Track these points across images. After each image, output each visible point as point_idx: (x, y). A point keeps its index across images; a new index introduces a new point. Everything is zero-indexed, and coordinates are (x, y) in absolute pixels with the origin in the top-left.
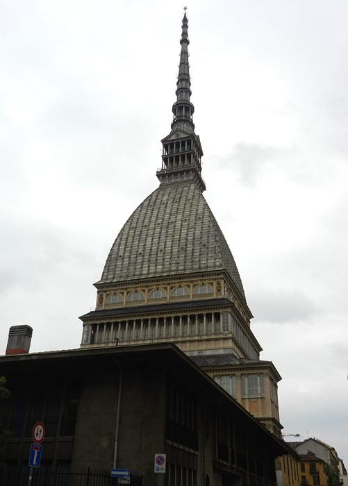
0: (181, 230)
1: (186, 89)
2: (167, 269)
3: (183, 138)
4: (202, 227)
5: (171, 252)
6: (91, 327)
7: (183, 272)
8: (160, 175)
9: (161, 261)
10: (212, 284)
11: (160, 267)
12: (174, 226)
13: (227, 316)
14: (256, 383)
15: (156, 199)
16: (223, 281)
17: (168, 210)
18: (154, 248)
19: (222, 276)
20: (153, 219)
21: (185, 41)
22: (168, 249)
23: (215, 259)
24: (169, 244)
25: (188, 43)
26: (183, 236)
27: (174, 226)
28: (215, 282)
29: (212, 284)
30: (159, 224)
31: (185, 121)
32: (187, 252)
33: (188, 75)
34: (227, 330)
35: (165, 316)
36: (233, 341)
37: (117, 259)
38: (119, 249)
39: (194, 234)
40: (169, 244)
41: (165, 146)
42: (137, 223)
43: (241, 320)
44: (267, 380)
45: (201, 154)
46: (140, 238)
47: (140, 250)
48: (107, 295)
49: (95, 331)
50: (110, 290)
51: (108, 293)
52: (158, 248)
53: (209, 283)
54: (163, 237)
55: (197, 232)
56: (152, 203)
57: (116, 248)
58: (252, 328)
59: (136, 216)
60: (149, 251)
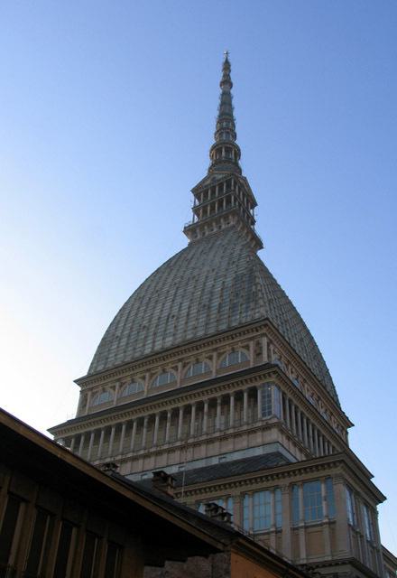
8: (189, 230)
10: (247, 347)
16: (265, 341)
20: (169, 280)
21: (227, 82)
24: (186, 304)
28: (252, 344)
29: (247, 347)
33: (231, 115)
34: (270, 413)
45: (254, 204)
48: (93, 394)
50: (97, 387)
54: (178, 300)
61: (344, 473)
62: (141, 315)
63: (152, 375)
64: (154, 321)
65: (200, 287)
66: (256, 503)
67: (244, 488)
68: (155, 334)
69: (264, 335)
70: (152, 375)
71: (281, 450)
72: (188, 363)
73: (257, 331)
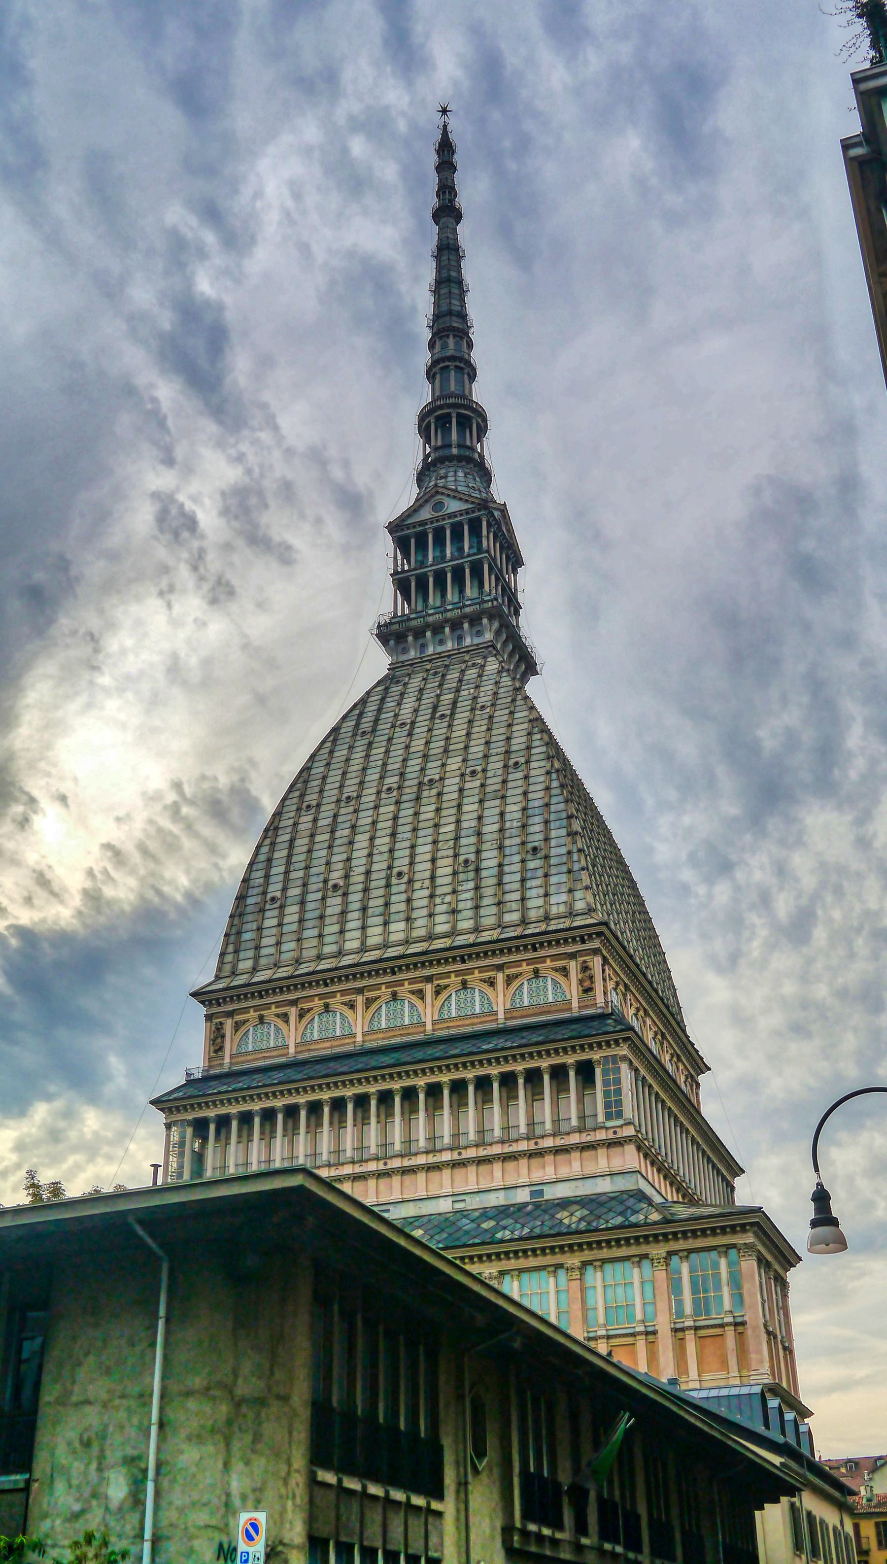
0: (459, 806)
1: (461, 359)
2: (422, 932)
4: (525, 793)
5: (433, 878)
6: (189, 1131)
7: (471, 938)
9: (403, 907)
10: (564, 971)
11: (398, 929)
12: (440, 794)
13: (618, 1070)
14: (717, 1276)
15: (380, 710)
16: (597, 961)
17: (418, 745)
18: (381, 864)
19: (596, 944)
20: (373, 776)
22: (423, 868)
23: (570, 891)
24: (424, 851)
25: (458, 216)
26: (469, 822)
27: (440, 794)
28: (573, 966)
29: (564, 971)
30: (389, 789)
31: (460, 459)
32: (484, 873)
34: (620, 1114)
35: (421, 1082)
36: (639, 1148)
37: (262, 911)
38: (267, 876)
39: (502, 814)
40: (424, 851)
41: (402, 544)
42: (321, 791)
43: (668, 1082)
44: (749, 1265)
45: (516, 561)
46: (333, 839)
47: (336, 876)
48: (237, 1026)
49: (205, 1139)
51: (238, 1018)
52: (390, 868)
53: (556, 970)
54: (404, 831)
55: (509, 808)
56: (366, 724)
57: (258, 876)
58: (709, 1110)
59: (318, 769)
60: (361, 878)
61: (757, 1243)
62: (321, 853)
63: (369, 1003)
64: (357, 878)
65: (449, 813)
66: (609, 1281)
67: (587, 1255)
68: (364, 909)
69: (596, 952)
70: (369, 1003)
71: (643, 1186)
72: (446, 987)
73: (583, 941)
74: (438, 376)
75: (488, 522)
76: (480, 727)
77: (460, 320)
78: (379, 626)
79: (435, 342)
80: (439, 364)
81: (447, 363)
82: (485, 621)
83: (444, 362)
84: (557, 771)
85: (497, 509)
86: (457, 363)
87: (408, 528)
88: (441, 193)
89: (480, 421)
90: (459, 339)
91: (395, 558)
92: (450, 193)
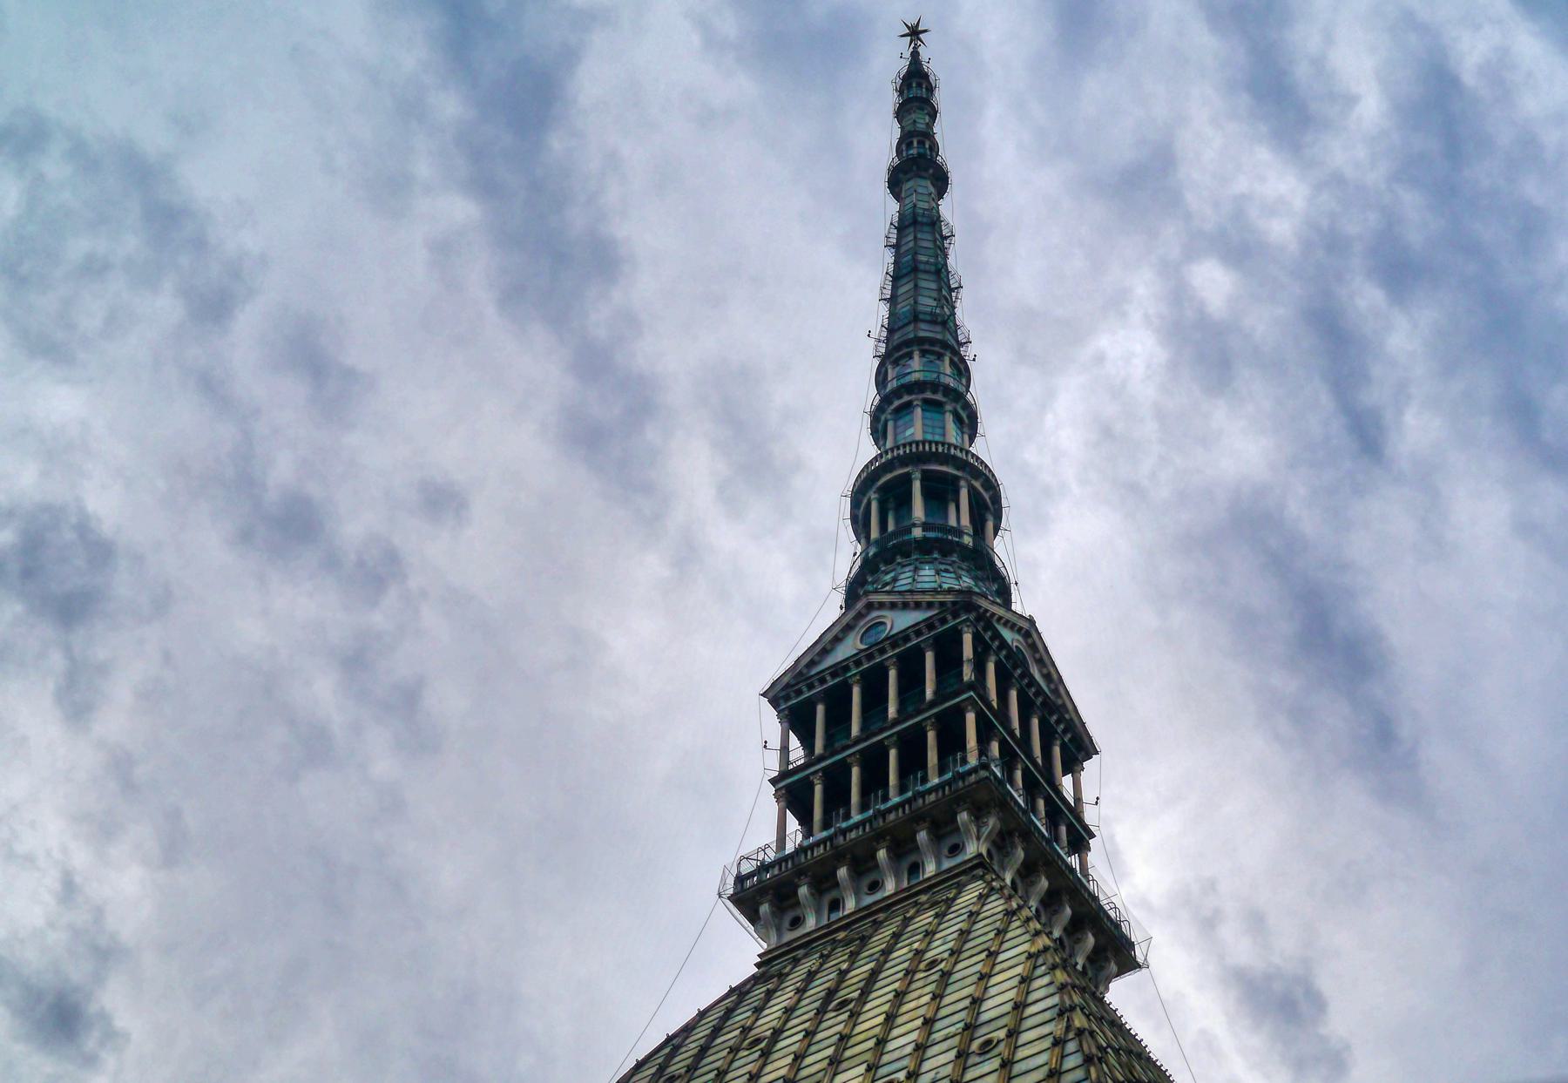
3: (904, 636)
25: (941, 181)
31: (925, 549)
33: (947, 322)
41: (797, 719)
45: (1079, 749)
74: (890, 425)
75: (977, 639)
76: (918, 1001)
77: (939, 328)
78: (740, 879)
79: (886, 372)
80: (891, 403)
81: (906, 398)
82: (963, 817)
83: (900, 397)
84: (1080, 1032)
85: (1012, 627)
86: (929, 395)
87: (811, 687)
88: (904, 147)
89: (977, 484)
90: (932, 357)
91: (785, 749)
92: (921, 143)
